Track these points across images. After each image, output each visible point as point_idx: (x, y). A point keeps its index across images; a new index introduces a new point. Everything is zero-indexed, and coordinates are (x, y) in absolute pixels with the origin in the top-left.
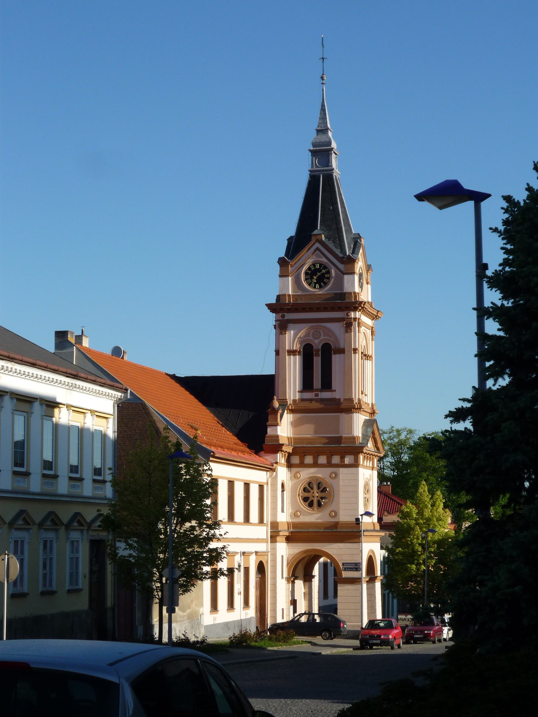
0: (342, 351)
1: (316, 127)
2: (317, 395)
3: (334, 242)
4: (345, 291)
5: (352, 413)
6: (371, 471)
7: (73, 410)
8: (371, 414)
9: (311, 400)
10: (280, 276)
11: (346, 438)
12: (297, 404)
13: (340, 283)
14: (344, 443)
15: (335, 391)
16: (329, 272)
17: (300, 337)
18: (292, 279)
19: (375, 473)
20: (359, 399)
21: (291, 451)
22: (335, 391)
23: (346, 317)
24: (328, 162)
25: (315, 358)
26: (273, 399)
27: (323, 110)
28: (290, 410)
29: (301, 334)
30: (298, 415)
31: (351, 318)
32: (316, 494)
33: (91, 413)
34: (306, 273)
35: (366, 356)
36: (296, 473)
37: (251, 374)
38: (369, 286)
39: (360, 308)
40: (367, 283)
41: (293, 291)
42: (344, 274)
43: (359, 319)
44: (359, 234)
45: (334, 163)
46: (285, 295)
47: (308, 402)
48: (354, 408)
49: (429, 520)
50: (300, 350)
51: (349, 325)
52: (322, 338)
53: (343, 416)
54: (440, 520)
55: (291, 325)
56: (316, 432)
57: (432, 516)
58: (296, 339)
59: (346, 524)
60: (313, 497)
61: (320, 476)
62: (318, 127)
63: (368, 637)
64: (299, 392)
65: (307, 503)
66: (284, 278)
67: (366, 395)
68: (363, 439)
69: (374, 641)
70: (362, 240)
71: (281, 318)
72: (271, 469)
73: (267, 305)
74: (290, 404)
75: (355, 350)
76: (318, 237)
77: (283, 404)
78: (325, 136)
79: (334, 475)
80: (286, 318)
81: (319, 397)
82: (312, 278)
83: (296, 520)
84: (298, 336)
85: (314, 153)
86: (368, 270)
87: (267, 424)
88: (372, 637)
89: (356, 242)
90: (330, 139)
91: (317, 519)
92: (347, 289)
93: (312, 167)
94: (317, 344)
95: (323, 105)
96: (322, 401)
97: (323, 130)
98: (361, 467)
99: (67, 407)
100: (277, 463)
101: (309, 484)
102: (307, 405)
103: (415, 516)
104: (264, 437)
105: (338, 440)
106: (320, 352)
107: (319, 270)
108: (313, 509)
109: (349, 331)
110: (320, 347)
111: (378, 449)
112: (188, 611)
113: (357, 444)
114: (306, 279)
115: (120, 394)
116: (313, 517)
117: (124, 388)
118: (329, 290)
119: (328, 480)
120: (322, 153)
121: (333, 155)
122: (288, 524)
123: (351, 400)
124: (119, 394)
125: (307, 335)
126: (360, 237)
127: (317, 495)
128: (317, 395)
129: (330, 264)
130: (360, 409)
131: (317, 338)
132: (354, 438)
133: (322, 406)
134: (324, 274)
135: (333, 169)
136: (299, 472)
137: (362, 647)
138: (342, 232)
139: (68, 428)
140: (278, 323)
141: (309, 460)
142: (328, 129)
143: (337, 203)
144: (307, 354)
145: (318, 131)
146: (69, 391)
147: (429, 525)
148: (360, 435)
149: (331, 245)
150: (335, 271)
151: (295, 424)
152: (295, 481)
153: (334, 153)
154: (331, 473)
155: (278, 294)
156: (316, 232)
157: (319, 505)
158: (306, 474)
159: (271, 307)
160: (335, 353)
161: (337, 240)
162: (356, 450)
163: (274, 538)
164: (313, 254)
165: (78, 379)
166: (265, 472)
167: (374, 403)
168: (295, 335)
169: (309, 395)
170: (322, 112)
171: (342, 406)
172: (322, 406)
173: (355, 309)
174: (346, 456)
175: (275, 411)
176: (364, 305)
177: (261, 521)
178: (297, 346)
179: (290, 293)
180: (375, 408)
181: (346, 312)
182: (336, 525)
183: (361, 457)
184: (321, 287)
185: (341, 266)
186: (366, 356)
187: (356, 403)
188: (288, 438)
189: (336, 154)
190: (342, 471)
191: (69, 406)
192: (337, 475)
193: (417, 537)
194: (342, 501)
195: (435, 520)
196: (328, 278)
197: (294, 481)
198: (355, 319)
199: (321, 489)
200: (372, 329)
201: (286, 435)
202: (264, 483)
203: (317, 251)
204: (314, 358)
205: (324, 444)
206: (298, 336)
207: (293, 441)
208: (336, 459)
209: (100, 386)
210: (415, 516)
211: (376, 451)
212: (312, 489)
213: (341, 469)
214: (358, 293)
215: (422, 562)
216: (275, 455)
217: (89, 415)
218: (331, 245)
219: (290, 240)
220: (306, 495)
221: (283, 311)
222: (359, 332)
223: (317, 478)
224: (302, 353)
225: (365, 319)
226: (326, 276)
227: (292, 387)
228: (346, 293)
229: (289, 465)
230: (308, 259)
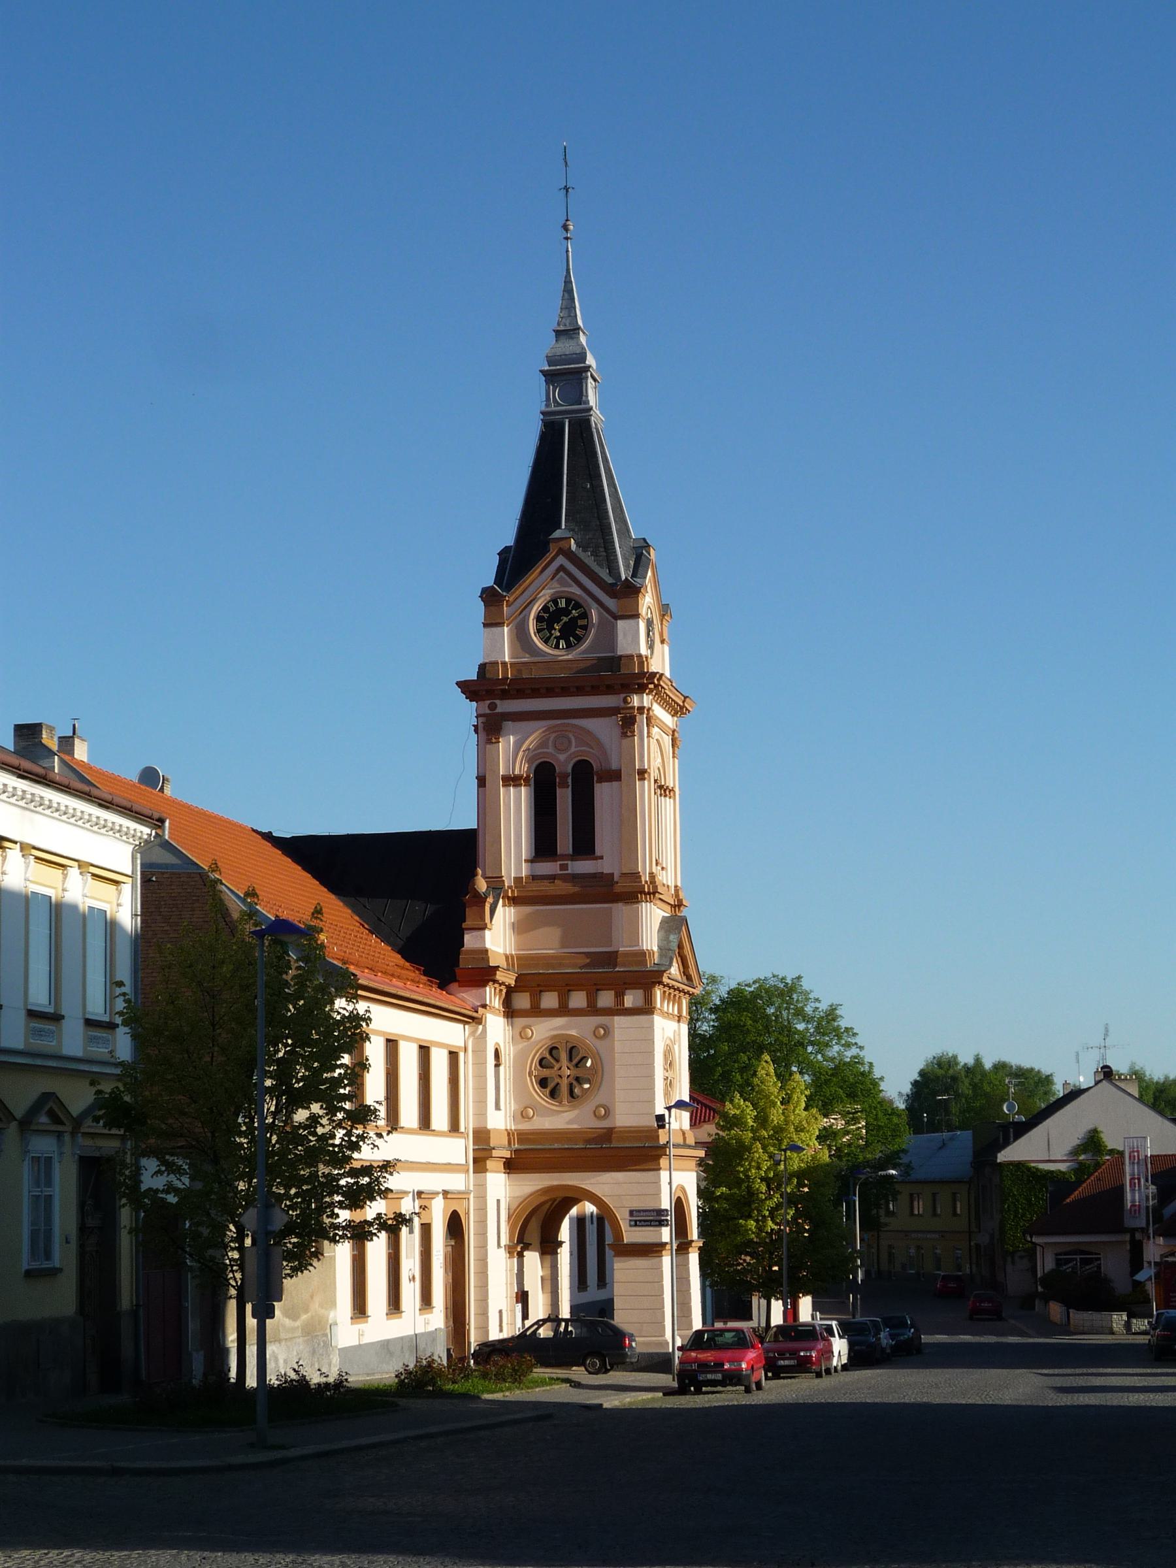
0: (614, 776)
1: (555, 326)
3: (595, 554)
4: (619, 653)
5: (638, 902)
6: (676, 1024)
7: (37, 858)
9: (552, 878)
10: (485, 625)
11: (626, 954)
12: (524, 887)
13: (609, 636)
14: (624, 965)
15: (601, 858)
16: (585, 615)
17: (528, 749)
18: (510, 631)
19: (684, 1028)
21: (513, 983)
22: (601, 858)
23: (622, 705)
26: (475, 875)
27: (568, 290)
28: (508, 898)
29: (531, 742)
30: (527, 909)
33: (80, 867)
34: (539, 619)
35: (664, 790)
36: (524, 1028)
38: (666, 648)
39: (651, 686)
40: (662, 642)
41: (511, 657)
42: (616, 618)
43: (649, 709)
44: (644, 539)
45: (592, 398)
47: (546, 882)
49: (779, 1130)
50: (528, 776)
51: (628, 722)
52: (573, 749)
53: (620, 909)
54: (802, 1130)
55: (508, 725)
57: (787, 1122)
58: (521, 754)
61: (573, 1033)
62: (559, 324)
63: (695, 1366)
65: (548, 1091)
66: (494, 629)
67: (663, 868)
68: (661, 956)
69: (709, 1376)
71: (488, 711)
72: (473, 1018)
73: (459, 684)
75: (642, 773)
76: (563, 544)
77: (496, 884)
78: (572, 343)
79: (602, 1032)
80: (499, 710)
81: (569, 871)
82: (550, 628)
83: (526, 1126)
84: (524, 747)
87: (464, 926)
88: (704, 1366)
89: (640, 554)
90: (583, 348)
91: (568, 1123)
92: (623, 648)
93: (547, 406)
94: (564, 762)
95: (568, 282)
96: (575, 878)
97: (568, 332)
99: (22, 849)
100: (484, 1006)
101: (552, 1050)
103: (750, 1122)
105: (611, 958)
107: (565, 612)
108: (560, 1103)
110: (569, 770)
111: (689, 978)
112: (304, 1317)
113: (649, 966)
114: (539, 631)
115: (147, 830)
116: (560, 1119)
117: (156, 816)
118: (584, 652)
119: (590, 1041)
120: (567, 376)
121: (590, 380)
122: (509, 1134)
123: (636, 876)
124: (145, 831)
125: (543, 744)
126: (647, 546)
129: (589, 600)
130: (654, 893)
131: (560, 751)
132: (642, 955)
133: (577, 889)
134: (574, 619)
135: (591, 409)
136: (529, 1027)
137: (682, 1390)
139: (26, 901)
141: (550, 1000)
142: (579, 328)
143: (600, 476)
144: (543, 782)
145: (559, 334)
146: (28, 813)
147: (780, 1141)
148: (655, 949)
149: (588, 558)
151: (519, 928)
152: (523, 1044)
155: (481, 662)
156: (557, 534)
157: (571, 1093)
158: (544, 1030)
159: (467, 688)
160: (600, 781)
162: (647, 979)
165: (48, 786)
166: (461, 1026)
167: (679, 884)
169: (548, 868)
171: (618, 889)
172: (577, 889)
173: (641, 689)
174: (627, 991)
175: (480, 900)
177: (454, 1127)
178: (521, 768)
179: (507, 659)
181: (623, 696)
182: (609, 1133)
183: (658, 992)
184: (569, 646)
185: (610, 603)
186: (664, 790)
188: (507, 957)
189: (595, 380)
190: (619, 1021)
191: (25, 848)
192: (608, 1031)
193: (759, 1164)
194: (619, 1083)
195: (792, 1129)
196: (585, 628)
197: (520, 1046)
198: (641, 709)
199: (575, 1062)
201: (501, 951)
202: (459, 1047)
203: (561, 573)
204: (558, 790)
205: (581, 968)
206: (524, 747)
207: (519, 962)
208: (606, 999)
209: (101, 805)
210: (750, 1122)
212: (557, 1061)
213: (616, 1018)
216: (481, 990)
217: (74, 872)
218: (588, 558)
219: (504, 554)
220: (546, 1073)
222: (648, 736)
223: (567, 1039)
225: (659, 711)
226: (580, 622)
227: (512, 852)
228: (621, 657)
229: (510, 1012)
230: (542, 589)
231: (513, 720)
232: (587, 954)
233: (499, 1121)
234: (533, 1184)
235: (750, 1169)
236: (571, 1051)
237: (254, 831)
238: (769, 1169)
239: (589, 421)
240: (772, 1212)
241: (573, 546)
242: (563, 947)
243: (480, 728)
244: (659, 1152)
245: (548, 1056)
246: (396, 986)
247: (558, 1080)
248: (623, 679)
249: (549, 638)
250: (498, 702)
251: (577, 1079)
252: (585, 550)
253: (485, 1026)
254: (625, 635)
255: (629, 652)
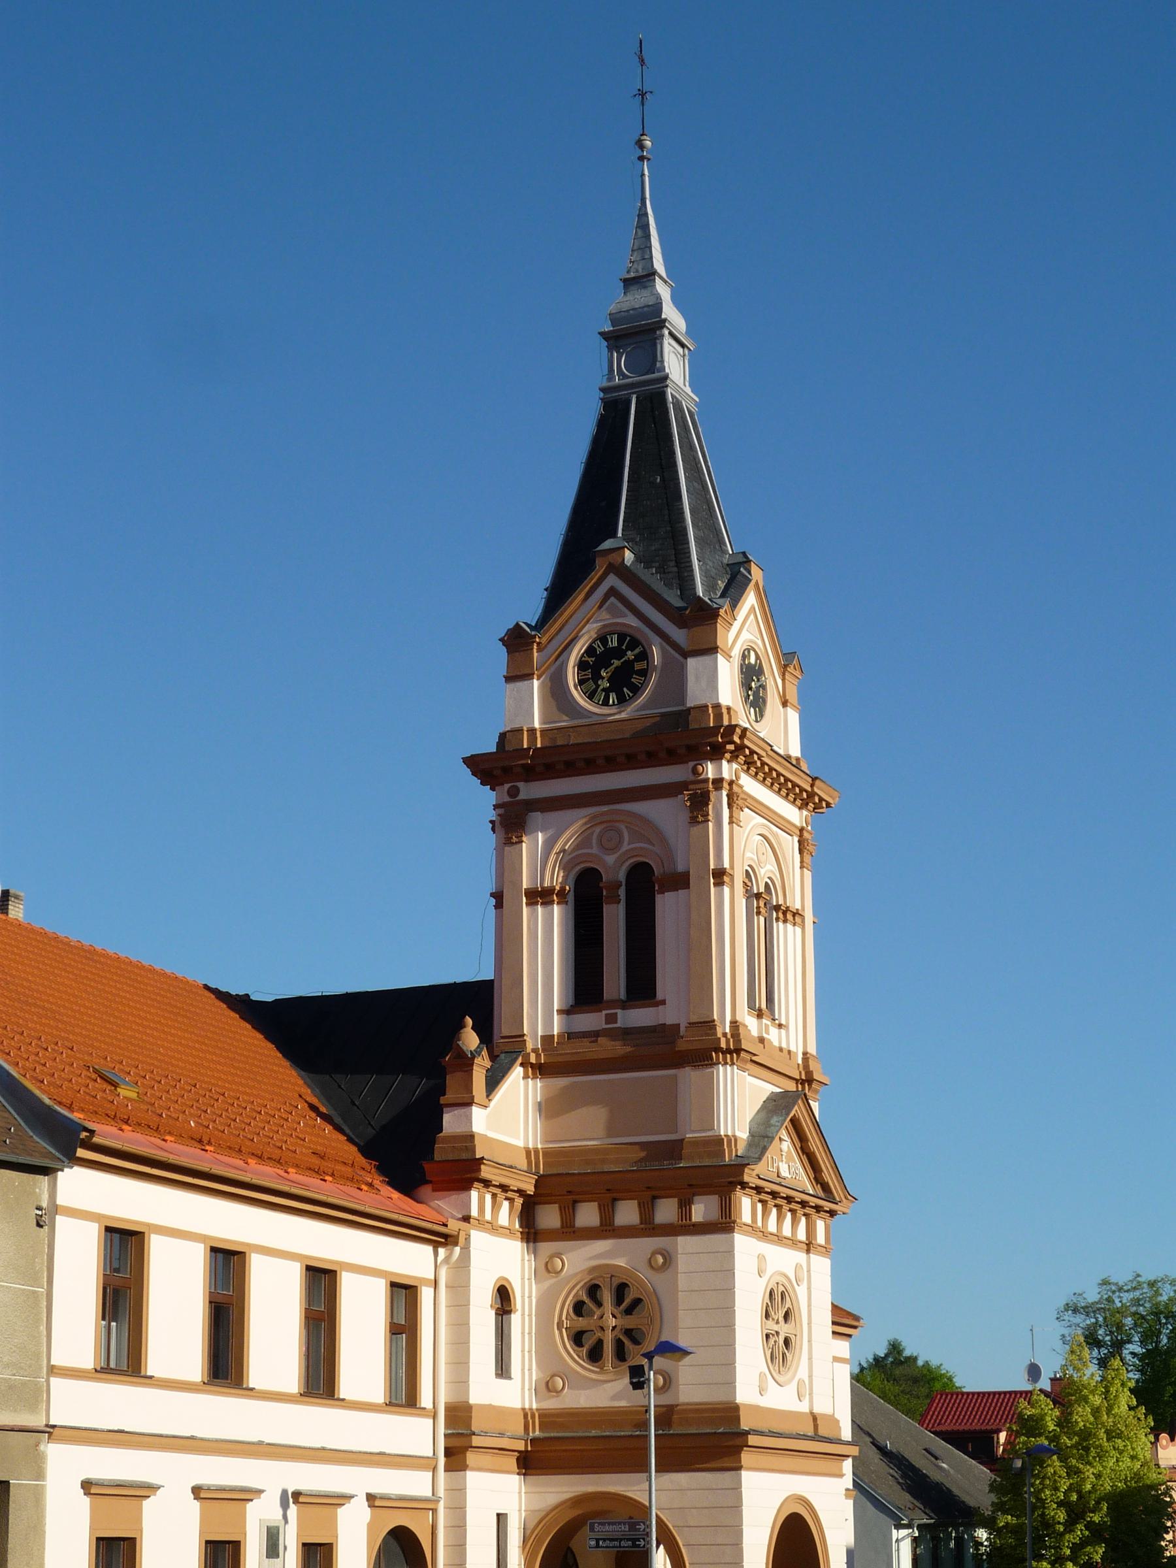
2: (611, 1019)
3: (662, 570)
4: (690, 703)
5: (713, 1065)
6: (803, 1255)
8: (803, 1082)
9: (594, 1035)
11: (696, 1143)
13: (676, 681)
15: (663, 1002)
16: (644, 656)
17: (564, 851)
18: (541, 687)
20: (735, 1024)
21: (531, 1190)
22: (663, 1002)
23: (692, 778)
24: (653, 360)
25: (607, 909)
26: (462, 1026)
28: (532, 1065)
29: (567, 840)
30: (561, 1082)
31: (706, 780)
32: (610, 1319)
34: (582, 665)
36: (552, 1257)
37: (451, 981)
38: (793, 717)
39: (731, 747)
40: (785, 704)
42: (686, 655)
43: (731, 783)
44: (744, 554)
46: (520, 730)
48: (718, 1049)
49: (1086, 1435)
50: (563, 889)
51: (699, 802)
52: (625, 847)
53: (689, 1076)
54: (1119, 1436)
55: (536, 817)
56: (611, 1131)
59: (697, 1410)
60: (602, 1328)
61: (621, 1262)
64: (560, 1012)
65: (585, 1350)
67: (780, 1026)
70: (754, 569)
71: (507, 799)
72: (446, 1236)
74: (535, 1050)
75: (720, 875)
76: (612, 558)
79: (660, 1260)
80: (522, 796)
81: (618, 1025)
82: (597, 677)
83: (552, 1404)
84: (557, 848)
85: (615, 339)
86: (786, 666)
87: (443, 1100)
91: (613, 1398)
92: (695, 696)
94: (613, 867)
96: (627, 1033)
98: (745, 1233)
100: (467, 1219)
101: (593, 1290)
102: (585, 1049)
103: (1051, 1426)
104: (433, 1142)
105: (674, 1149)
106: (622, 892)
107: (618, 653)
108: (602, 1369)
109: (700, 819)
110: (622, 876)
111: (825, 1187)
116: (605, 1392)
118: (643, 707)
119: (644, 1274)
122: (525, 1416)
123: (709, 1025)
125: (583, 842)
127: (613, 1322)
128: (611, 1019)
132: (717, 1143)
133: (629, 1049)
134: (630, 664)
136: (558, 1255)
138: (686, 542)
140: (501, 811)
144: (586, 898)
150: (664, 653)
151: (549, 1109)
152: (550, 1282)
153: (671, 334)
154: (654, 1253)
156: (608, 544)
157: (620, 1354)
158: (580, 1259)
159: (484, 768)
161: (672, 563)
163: (456, 1454)
164: (600, 607)
166: (429, 1249)
167: (812, 1050)
168: (549, 844)
169: (591, 1021)
170: (640, 232)
171: (682, 1046)
172: (629, 1049)
173: (716, 753)
174: (696, 1198)
175: (465, 1062)
176: (742, 737)
177: (404, 1395)
178: (554, 878)
179: (537, 725)
180: (813, 1066)
181: (691, 764)
185: (679, 635)
186: (767, 906)
187: (725, 1035)
190: (685, 1244)
192: (669, 1259)
193: (1055, 1483)
195: (1102, 1434)
196: (644, 673)
200: (801, 836)
201: (520, 1143)
202: (425, 1281)
203: (612, 599)
204: (605, 907)
206: (557, 848)
210: (1051, 1426)
211: (821, 1193)
212: (599, 1304)
213: (680, 1239)
214: (729, 709)
215: (1068, 1552)
216: (463, 1195)
220: (582, 1323)
221: (514, 774)
222: (731, 822)
223: (612, 1271)
224: (571, 898)
226: (638, 666)
227: (541, 1002)
228: (689, 709)
229: (531, 1233)
230: (586, 626)
231: (543, 810)
232: (643, 1145)
233: (489, 1392)
234: (560, 1490)
235: (1042, 1490)
236: (621, 1291)
237: (206, 987)
238: (1070, 1489)
239: (663, 394)
240: (1076, 1549)
241: (629, 556)
242: (609, 1136)
243: (497, 825)
244: (738, 1442)
245: (585, 1298)
246: (365, 1200)
247: (599, 1334)
248: (693, 740)
249: (595, 691)
250: (521, 785)
251: (628, 1332)
252: (647, 567)
253: (466, 1249)
254: (697, 678)
255: (703, 702)
